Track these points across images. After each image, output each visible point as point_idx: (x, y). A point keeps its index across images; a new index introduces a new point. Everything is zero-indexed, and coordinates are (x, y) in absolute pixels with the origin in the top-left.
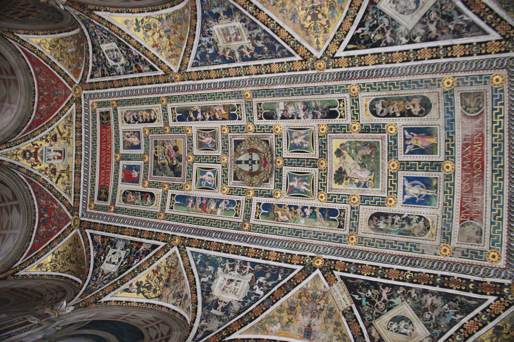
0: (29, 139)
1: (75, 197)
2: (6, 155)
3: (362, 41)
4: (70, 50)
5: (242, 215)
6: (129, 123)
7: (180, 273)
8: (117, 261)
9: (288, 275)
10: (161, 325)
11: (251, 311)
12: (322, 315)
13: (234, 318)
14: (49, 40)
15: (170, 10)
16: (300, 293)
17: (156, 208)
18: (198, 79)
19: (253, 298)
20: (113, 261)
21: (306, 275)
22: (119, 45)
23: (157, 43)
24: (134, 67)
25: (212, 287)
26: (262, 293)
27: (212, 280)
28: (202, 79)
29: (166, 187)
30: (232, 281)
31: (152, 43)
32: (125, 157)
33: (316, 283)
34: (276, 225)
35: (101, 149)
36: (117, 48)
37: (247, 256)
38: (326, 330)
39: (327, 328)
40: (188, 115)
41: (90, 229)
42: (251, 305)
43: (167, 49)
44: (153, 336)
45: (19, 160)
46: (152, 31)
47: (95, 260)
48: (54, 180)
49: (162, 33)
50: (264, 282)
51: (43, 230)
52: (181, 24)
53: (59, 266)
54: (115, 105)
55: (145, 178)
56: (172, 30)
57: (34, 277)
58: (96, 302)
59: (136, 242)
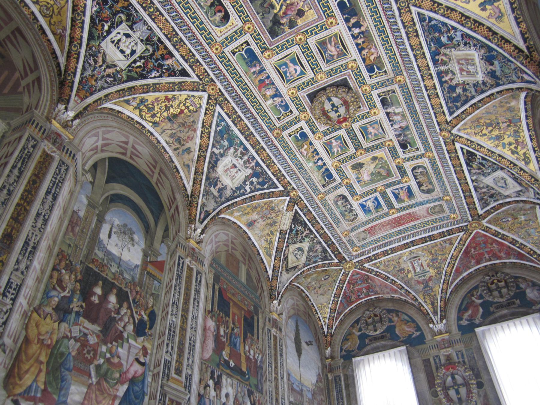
3: (470, 158)
5: (283, 123)
8: (128, 52)
9: (271, 188)
11: (236, 202)
19: (241, 191)
20: (122, 46)
25: (218, 162)
26: (249, 190)
27: (222, 155)
30: (235, 166)
37: (258, 154)
39: (263, 230)
42: (238, 196)
50: (255, 183)
59: (166, 48)
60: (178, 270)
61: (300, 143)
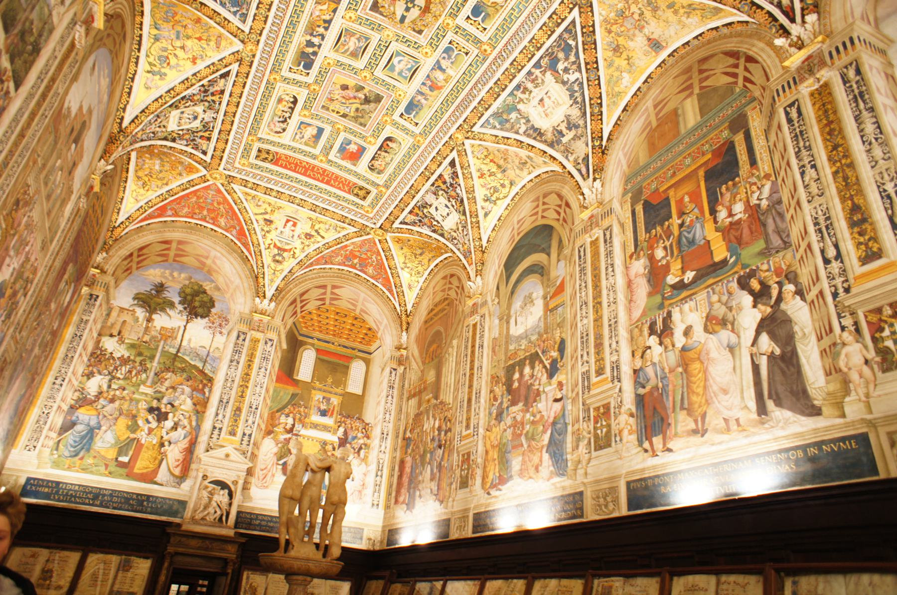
0: (260, 251)
1: (350, 224)
2: (272, 281)
4: (157, 167)
6: (284, 130)
7: (498, 151)
8: (447, 210)
10: (546, 200)
11: (591, 99)
12: (648, 17)
13: (586, 122)
14: (134, 187)
15: (147, 20)
16: (606, 29)
17: (406, 142)
18: (265, 22)
19: (576, 88)
21: (589, 9)
22: (177, 107)
23: (191, 57)
24: (213, 98)
25: (536, 126)
26: (577, 75)
27: (528, 121)
28: (267, 17)
29: (388, 119)
30: (542, 100)
31: (189, 64)
32: (327, 150)
33: (607, 3)
34: (506, 12)
35: (304, 174)
36: (179, 111)
37: (523, 67)
38: (667, 22)
40: (308, 54)
41: (394, 222)
42: (583, 94)
43: (205, 46)
44: (556, 216)
45: (282, 270)
46: (170, 56)
47: (434, 231)
48: (319, 239)
49: (178, 44)
50: (566, 64)
51: (370, 270)
52: (176, 13)
53: (420, 269)
54: (255, 138)
55: (364, 138)
56: (179, 28)
57: (419, 297)
58: (484, 252)
59: (436, 180)
60: (580, 265)
61: (490, 10)
